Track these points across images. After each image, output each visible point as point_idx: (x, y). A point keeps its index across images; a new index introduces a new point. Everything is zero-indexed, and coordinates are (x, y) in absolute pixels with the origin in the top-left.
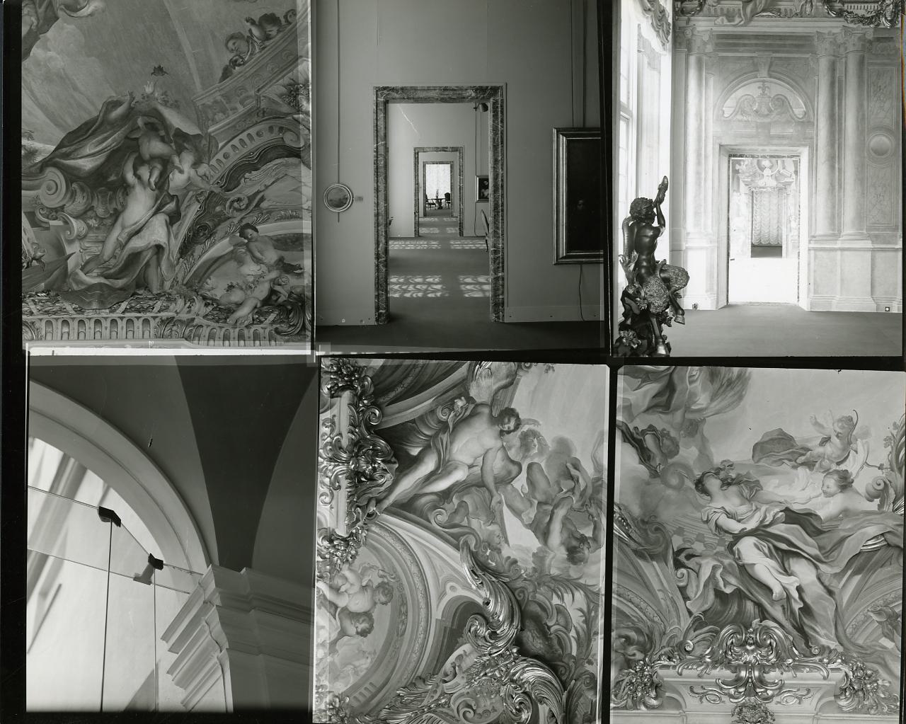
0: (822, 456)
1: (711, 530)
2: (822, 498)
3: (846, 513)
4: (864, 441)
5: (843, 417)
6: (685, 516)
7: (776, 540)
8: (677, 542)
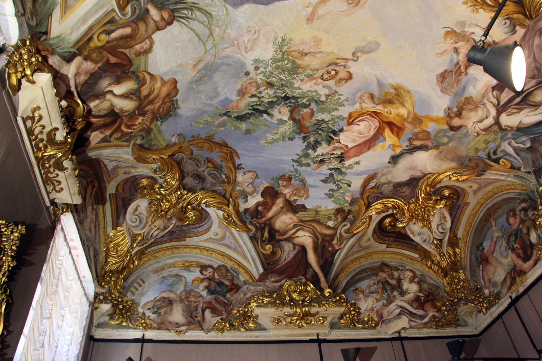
4: (467, 26)
6: (469, 144)
8: (482, 154)
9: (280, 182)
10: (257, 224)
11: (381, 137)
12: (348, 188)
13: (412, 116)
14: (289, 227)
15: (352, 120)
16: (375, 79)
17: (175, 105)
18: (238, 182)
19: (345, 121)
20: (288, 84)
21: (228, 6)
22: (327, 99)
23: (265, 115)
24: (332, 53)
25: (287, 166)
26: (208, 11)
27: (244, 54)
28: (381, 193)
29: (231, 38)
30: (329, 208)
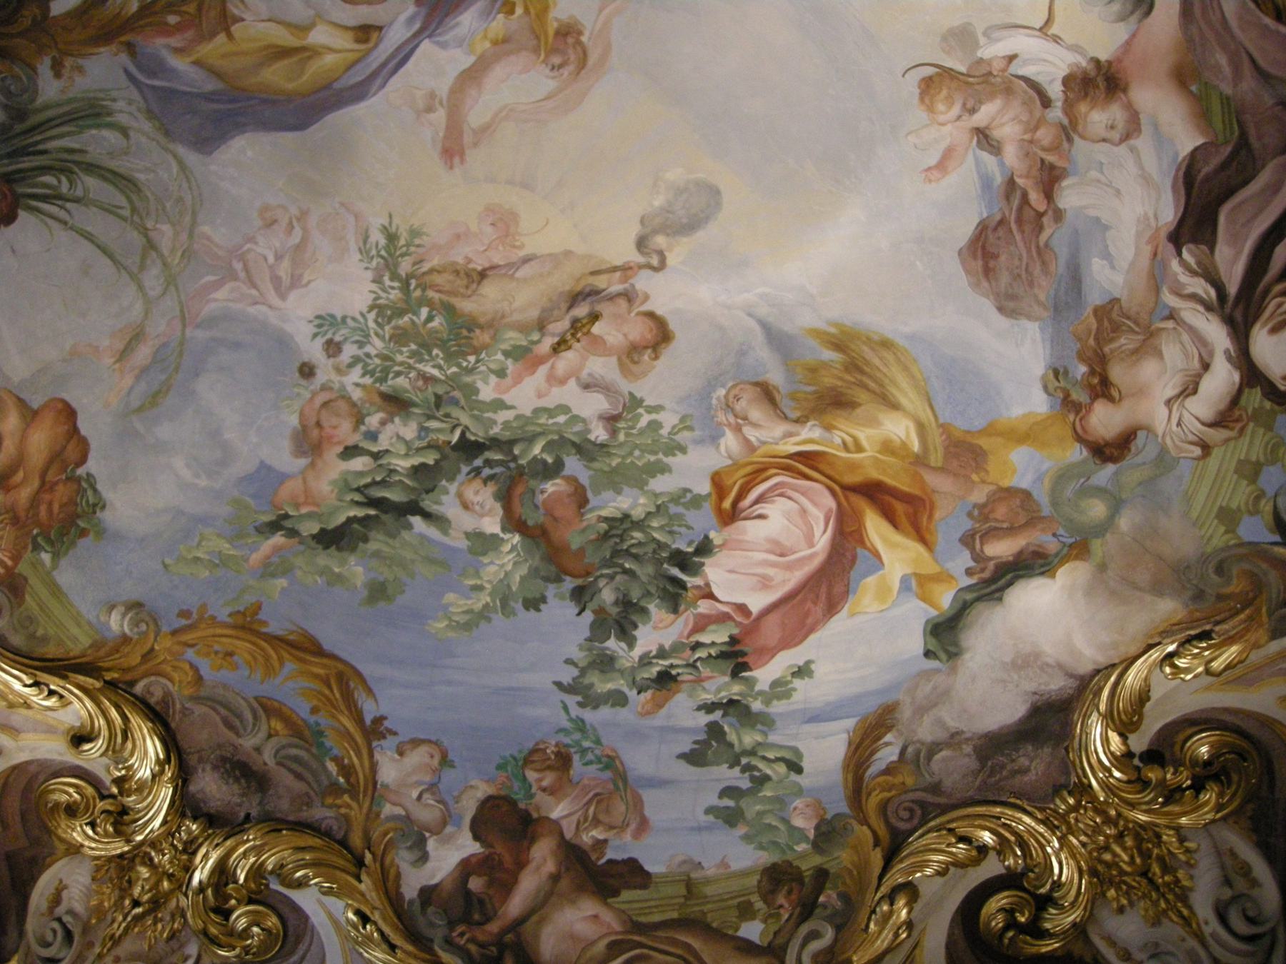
0: (1028, 146)
1: (1227, 441)
2: (1143, 143)
3: (1185, 76)
4: (982, 40)
5: (922, 99)
6: (1188, 499)
7: (1265, 271)
9: (531, 775)
10: (473, 948)
11: (860, 551)
12: (794, 777)
13: (937, 439)
14: (589, 954)
15: (731, 500)
16: (752, 323)
17: (90, 493)
18: (386, 787)
19: (708, 507)
20: (457, 394)
21: (181, 150)
22: (614, 433)
23: (416, 521)
24: (568, 254)
25: (540, 712)
26: (121, 171)
27: (275, 301)
28: (935, 788)
29: (220, 253)
30: (736, 866)
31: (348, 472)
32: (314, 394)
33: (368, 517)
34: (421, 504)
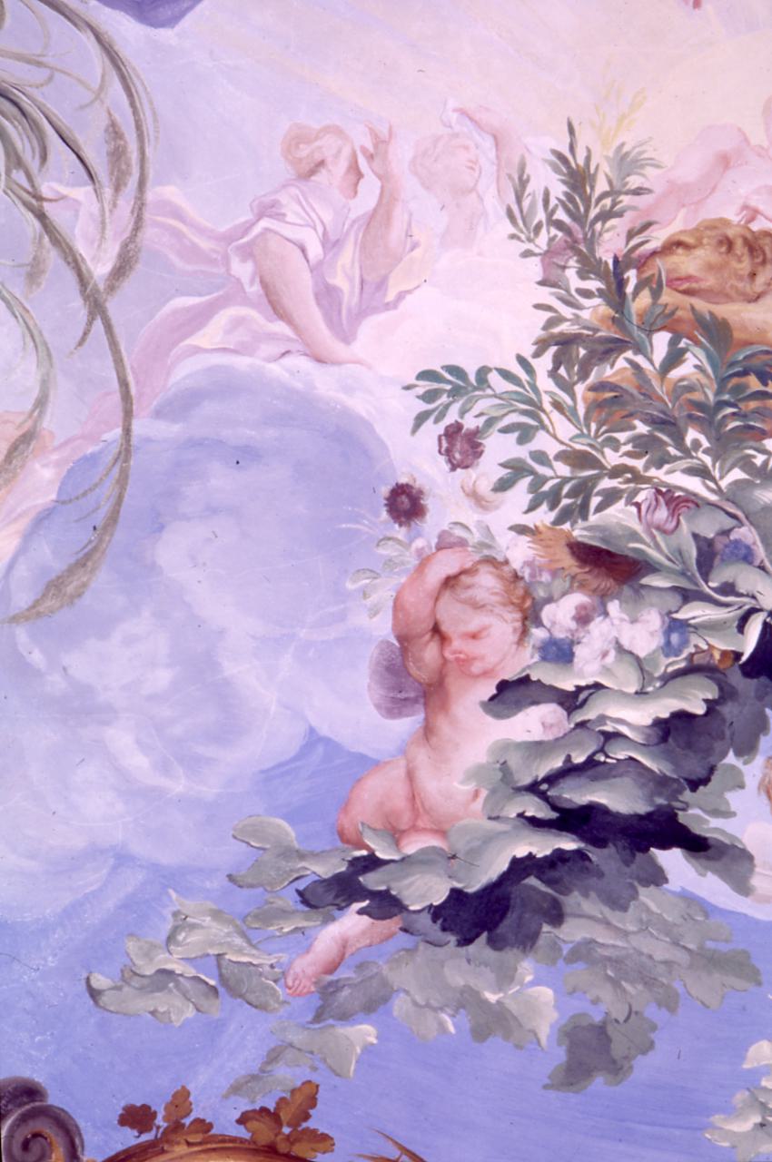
23: (671, 859)
31: (507, 746)
32: (424, 562)
33: (559, 857)
34: (682, 818)
